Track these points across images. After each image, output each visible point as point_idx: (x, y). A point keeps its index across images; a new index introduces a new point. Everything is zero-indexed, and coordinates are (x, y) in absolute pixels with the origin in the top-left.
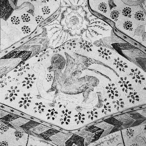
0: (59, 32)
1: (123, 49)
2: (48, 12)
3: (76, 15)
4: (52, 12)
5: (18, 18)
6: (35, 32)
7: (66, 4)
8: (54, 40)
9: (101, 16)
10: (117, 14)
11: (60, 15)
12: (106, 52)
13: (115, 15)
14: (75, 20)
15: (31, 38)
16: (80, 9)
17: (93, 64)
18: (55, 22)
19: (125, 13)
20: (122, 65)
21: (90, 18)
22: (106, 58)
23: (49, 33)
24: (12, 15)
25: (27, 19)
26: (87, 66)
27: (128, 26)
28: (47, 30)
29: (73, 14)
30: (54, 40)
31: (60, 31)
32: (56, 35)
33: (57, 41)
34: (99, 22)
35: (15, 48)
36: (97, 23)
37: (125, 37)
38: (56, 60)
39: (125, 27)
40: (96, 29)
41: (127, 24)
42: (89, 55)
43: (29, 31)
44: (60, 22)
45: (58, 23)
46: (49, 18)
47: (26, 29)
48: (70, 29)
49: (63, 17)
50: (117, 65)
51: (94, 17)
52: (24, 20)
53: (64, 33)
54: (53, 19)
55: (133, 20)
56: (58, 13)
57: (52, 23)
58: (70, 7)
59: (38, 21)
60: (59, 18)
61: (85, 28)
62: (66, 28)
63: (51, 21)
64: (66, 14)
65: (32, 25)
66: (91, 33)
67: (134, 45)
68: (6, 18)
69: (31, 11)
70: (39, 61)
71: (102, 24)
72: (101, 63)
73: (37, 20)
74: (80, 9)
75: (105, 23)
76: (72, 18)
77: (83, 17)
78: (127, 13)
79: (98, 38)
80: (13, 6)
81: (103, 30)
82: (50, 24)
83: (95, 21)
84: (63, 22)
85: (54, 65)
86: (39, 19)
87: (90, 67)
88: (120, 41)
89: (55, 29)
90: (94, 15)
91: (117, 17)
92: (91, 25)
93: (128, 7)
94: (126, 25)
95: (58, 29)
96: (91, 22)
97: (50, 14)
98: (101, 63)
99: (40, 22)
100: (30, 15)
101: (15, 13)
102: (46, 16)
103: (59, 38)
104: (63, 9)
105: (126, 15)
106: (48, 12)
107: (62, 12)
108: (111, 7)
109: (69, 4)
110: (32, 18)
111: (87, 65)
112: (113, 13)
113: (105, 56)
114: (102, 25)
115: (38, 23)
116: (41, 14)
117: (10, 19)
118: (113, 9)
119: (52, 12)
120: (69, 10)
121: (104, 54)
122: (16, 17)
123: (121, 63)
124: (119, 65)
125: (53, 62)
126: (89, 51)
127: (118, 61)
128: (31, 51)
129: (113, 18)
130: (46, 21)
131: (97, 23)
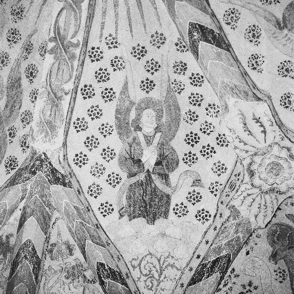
2: (223, 169)
3: (273, 159)
4: (230, 167)
5: (183, 205)
6: (218, 215)
7: (247, 152)
8: (256, 216)
11: (245, 172)
15: (218, 229)
16: (276, 148)
18: (243, 188)
23: (244, 211)
24: (172, 206)
25: (197, 197)
28: (236, 207)
29: (267, 161)
30: (256, 216)
31: (259, 196)
32: (256, 205)
33: (261, 216)
35: (201, 258)
38: (276, 235)
43: (208, 216)
45: (249, 186)
46: (230, 181)
47: (202, 216)
48: (275, 185)
49: (252, 174)
52: (193, 202)
53: (267, 196)
58: (256, 154)
59: (215, 193)
60: (247, 178)
62: (266, 187)
64: (254, 167)
65: (209, 203)
68: (166, 215)
69: (197, 182)
70: (248, 253)
73: (212, 192)
74: (276, 148)
76: (269, 167)
77: (286, 157)
80: (167, 190)
82: (236, 195)
84: (257, 181)
85: (277, 247)
86: (215, 188)
89: (250, 199)
95: (254, 196)
97: (228, 172)
99: (218, 193)
100: (197, 189)
101: (175, 200)
102: (223, 178)
103: (262, 207)
104: (246, 163)
106: (223, 170)
107: (246, 167)
109: (253, 151)
110: (205, 192)
115: (216, 195)
116: (214, 178)
117: (171, 211)
119: (230, 167)
120: (257, 159)
122: (179, 204)
125: (273, 243)
128: (227, 253)
130: (227, 189)
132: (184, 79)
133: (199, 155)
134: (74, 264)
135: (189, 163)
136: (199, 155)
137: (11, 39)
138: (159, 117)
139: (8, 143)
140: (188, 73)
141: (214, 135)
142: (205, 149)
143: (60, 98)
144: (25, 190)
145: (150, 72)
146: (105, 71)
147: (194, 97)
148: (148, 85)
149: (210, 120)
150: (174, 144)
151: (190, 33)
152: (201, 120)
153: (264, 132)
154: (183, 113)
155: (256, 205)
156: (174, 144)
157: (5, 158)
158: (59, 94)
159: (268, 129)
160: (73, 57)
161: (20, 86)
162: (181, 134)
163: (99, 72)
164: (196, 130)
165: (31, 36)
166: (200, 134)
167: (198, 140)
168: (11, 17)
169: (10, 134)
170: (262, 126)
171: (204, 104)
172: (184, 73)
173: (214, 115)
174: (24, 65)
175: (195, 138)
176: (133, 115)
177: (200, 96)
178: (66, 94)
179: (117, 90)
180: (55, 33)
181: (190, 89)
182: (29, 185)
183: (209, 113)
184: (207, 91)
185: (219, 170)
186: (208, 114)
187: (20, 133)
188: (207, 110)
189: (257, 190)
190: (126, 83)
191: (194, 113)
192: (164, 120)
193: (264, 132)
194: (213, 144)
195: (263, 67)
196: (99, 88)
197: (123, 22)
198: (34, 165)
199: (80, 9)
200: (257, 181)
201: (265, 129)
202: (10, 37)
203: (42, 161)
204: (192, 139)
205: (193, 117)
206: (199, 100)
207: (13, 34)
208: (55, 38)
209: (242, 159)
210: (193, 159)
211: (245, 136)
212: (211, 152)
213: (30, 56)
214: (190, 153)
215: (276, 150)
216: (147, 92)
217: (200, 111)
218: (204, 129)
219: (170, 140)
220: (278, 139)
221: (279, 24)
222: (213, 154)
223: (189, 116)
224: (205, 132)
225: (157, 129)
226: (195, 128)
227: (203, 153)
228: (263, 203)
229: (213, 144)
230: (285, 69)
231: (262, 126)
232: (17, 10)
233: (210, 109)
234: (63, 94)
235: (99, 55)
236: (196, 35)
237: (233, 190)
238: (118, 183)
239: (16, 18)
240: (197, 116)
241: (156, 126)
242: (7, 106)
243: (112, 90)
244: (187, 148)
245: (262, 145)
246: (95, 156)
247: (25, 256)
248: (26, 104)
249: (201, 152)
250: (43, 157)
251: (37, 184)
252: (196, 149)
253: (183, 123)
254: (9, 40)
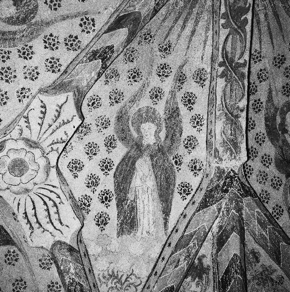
134: (261, 270)
137: (161, 74)
139: (176, 171)
143: (237, 117)
144: (219, 210)
157: (177, 186)
158: (235, 113)
160: (243, 75)
161: (178, 115)
165: (181, 67)
168: (158, 53)
169: (176, 162)
174: (179, 95)
176: (279, 120)
178: (242, 111)
179: (264, 99)
180: (223, 57)
182: (224, 203)
187: (187, 159)
198: (225, 183)
199: (244, 32)
202: (160, 72)
203: (231, 177)
207: (162, 69)
208: (224, 62)
213: (184, 86)
232: (165, 47)
234: (239, 112)
238: (280, 185)
239: (164, 54)
242: (167, 137)
246: (256, 165)
247: (236, 271)
248: (188, 130)
250: (232, 174)
251: (231, 200)
254: (160, 76)
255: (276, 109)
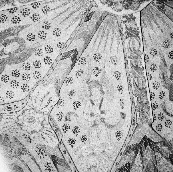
0: (11, 123)
1: (59, 164)
7: (32, 105)
9: (55, 125)
10: (68, 128)
11: (22, 111)
12: (43, 152)
13: (66, 128)
14: (32, 120)
16: (42, 115)
17: (26, 156)
19: (74, 131)
20: (51, 170)
21: (45, 126)
22: (41, 156)
26: (20, 155)
27: (72, 142)
29: (33, 115)
34: (51, 133)
36: (50, 132)
37: (65, 152)
39: (69, 142)
40: (46, 136)
41: (71, 141)
42: (27, 146)
44: (18, 117)
45: (16, 116)
48: (23, 125)
49: (23, 113)
50: (46, 168)
51: (49, 126)
54: (14, 109)
55: (77, 139)
56: (19, 104)
57: (10, 115)
61: (38, 131)
62: (20, 122)
63: (10, 112)
64: (27, 112)
66: (40, 137)
67: (68, 162)
71: (53, 135)
72: (33, 158)
74: (42, 115)
75: (56, 136)
78: (76, 131)
79: (43, 143)
81: (51, 140)
83: (48, 129)
87: (22, 157)
88: (58, 155)
90: (50, 125)
91: (66, 130)
92: (44, 131)
93: (79, 127)
94: (70, 141)
96: (45, 129)
98: (33, 158)
102: (7, 100)
104: (26, 107)
105: (74, 133)
107: (25, 109)
108: (67, 120)
109: (34, 107)
111: (21, 154)
112: (65, 125)
113: (40, 155)
114: (52, 137)
118: (67, 122)
120: (32, 111)
121: (40, 152)
123: (50, 168)
124: (48, 169)
126: (29, 142)
127: (49, 165)
129: (63, 130)
131: (50, 132)
132: (45, 54)
133: (10, 81)
135: (3, 79)
136: (10, 81)
138: (17, 52)
140: (49, 55)
141: (25, 82)
142: (15, 82)
145: (39, 36)
146: (28, 13)
147: (38, 63)
148: (31, 38)
149: (31, 76)
150: (7, 66)
151: (72, 51)
152: (28, 72)
153: (46, 106)
154: (27, 61)
155: (9, 124)
156: (7, 66)
159: (48, 107)
162: (14, 67)
163: (27, 10)
164: (21, 73)
166: (21, 76)
167: (17, 77)
170: (48, 104)
171: (37, 70)
172: (48, 53)
173: (35, 77)
175: (17, 74)
176: (11, 38)
177: (40, 66)
178: (13, 4)
179: (21, 23)
181: (41, 59)
183: (34, 74)
184: (45, 68)
185: (10, 95)
186: (33, 74)
188: (35, 72)
189: (16, 120)
190: (27, 26)
191: (30, 67)
192: (17, 54)
193: (46, 106)
194: (20, 84)
195: (69, 85)
196: (18, 14)
197: (58, 11)
200: (21, 118)
201: (47, 105)
204: (16, 73)
205: (28, 68)
206: (38, 66)
209: (27, 105)
210: (6, 80)
211: (39, 100)
212: (15, 86)
214: (8, 77)
215: (40, 115)
216: (27, 39)
217: (33, 69)
218: (25, 76)
219: (8, 63)
220: (45, 113)
221: (88, 81)
222: (15, 87)
223: (27, 66)
224: (23, 77)
225: (10, 54)
226: (22, 71)
227: (12, 83)
228: (12, 126)
229: (20, 84)
230: (72, 93)
231: (48, 104)
233: (36, 73)
234: (12, 3)
235: (36, 6)
236: (72, 54)
237: (9, 110)
240: (29, 69)
241: (12, 52)
243: (20, 21)
244: (9, 74)
245: (39, 109)
249: (12, 81)
252: (12, 78)
253: (21, 64)
255: (17, 34)
